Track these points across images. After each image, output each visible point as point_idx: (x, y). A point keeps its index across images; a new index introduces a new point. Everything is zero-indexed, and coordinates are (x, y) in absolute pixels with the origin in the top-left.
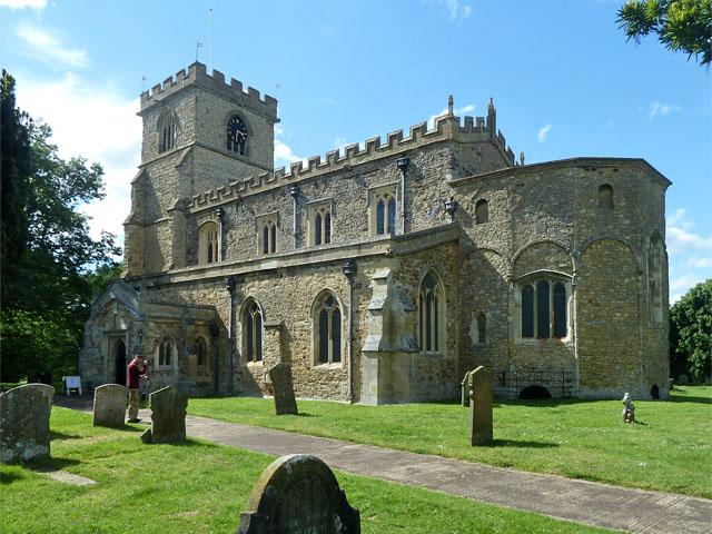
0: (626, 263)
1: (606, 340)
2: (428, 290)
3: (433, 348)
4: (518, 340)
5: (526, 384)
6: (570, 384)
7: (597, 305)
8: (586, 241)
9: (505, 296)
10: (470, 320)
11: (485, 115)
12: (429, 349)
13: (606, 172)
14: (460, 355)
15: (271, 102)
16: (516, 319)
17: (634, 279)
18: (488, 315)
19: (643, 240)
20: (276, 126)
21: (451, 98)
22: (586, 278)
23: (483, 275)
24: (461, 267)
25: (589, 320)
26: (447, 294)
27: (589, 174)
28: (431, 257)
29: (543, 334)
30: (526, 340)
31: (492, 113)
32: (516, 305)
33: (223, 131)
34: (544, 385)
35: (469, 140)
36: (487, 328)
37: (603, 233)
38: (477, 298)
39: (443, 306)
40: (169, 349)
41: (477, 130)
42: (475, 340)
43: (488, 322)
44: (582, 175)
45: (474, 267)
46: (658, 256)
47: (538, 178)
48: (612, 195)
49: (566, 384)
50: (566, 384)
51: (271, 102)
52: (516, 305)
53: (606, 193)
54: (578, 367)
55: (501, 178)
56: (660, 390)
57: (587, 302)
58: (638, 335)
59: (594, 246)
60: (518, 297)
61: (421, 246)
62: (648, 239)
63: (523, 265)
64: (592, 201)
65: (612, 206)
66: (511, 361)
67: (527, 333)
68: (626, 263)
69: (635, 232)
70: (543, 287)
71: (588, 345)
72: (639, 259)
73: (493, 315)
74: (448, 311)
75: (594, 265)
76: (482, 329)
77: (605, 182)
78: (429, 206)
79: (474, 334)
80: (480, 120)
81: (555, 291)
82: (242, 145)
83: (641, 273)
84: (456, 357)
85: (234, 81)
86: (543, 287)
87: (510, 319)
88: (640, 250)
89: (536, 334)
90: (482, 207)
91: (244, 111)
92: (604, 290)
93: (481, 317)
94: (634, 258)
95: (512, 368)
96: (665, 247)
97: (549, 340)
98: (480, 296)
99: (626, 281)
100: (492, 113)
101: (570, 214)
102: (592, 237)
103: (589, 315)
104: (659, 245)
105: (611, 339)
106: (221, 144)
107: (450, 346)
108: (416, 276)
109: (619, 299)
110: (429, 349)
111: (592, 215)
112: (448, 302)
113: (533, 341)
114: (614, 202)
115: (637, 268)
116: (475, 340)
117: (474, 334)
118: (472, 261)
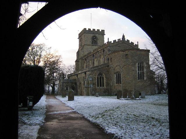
4: (116, 85)
11: (121, 38)
13: (127, 52)
15: (103, 31)
16: (115, 80)
20: (105, 36)
25: (124, 80)
31: (124, 36)
33: (91, 40)
39: (104, 78)
40: (68, 87)
42: (111, 85)
51: (103, 31)
67: (117, 83)
82: (96, 43)
85: (93, 29)
86: (118, 74)
91: (97, 35)
100: (124, 36)
106: (90, 44)
107: (107, 86)
110: (101, 86)
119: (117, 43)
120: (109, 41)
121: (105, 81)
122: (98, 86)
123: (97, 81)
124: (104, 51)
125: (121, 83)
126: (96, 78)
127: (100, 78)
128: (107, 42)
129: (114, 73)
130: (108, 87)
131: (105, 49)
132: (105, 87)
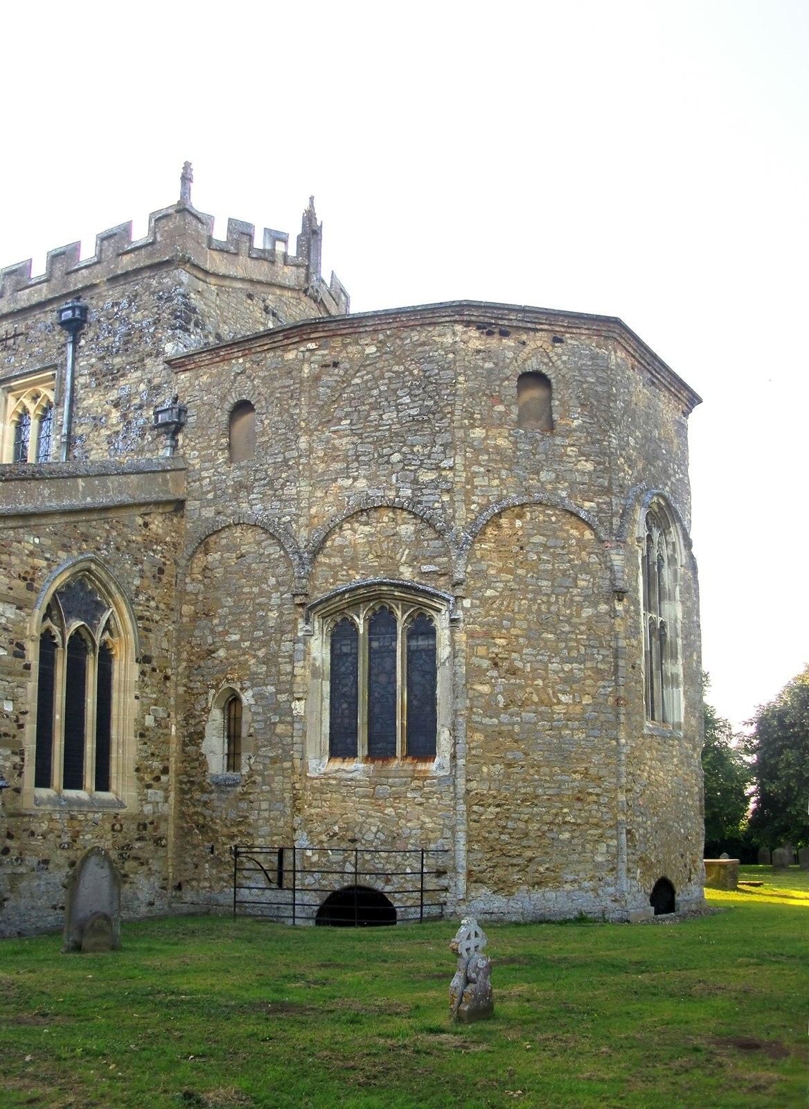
0: (585, 568)
1: (536, 766)
2: (76, 624)
3: (89, 779)
5: (335, 883)
6: (444, 882)
7: (513, 672)
8: (483, 508)
9: (287, 646)
10: (207, 711)
12: (73, 779)
13: (538, 341)
14: (181, 802)
17: (603, 608)
18: (247, 698)
19: (626, 514)
21: (187, 167)
22: (484, 601)
23: (236, 593)
24: (188, 571)
26: (142, 641)
27: (493, 342)
28: (86, 538)
29: (380, 751)
30: (337, 764)
32: (316, 673)
34: (379, 885)
35: (240, 273)
36: (244, 734)
37: (528, 491)
38: (222, 653)
39: (125, 670)
41: (267, 257)
42: (216, 764)
43: (246, 717)
44: (476, 344)
45: (219, 573)
46: (673, 560)
47: (371, 350)
48: (550, 398)
49: (431, 883)
50: (431, 883)
52: (316, 673)
53: (535, 394)
54: (461, 836)
55: (285, 348)
56: (678, 889)
57: (486, 664)
58: (617, 751)
59: (504, 521)
60: (320, 650)
61: (54, 504)
62: (640, 515)
63: (331, 567)
64: (501, 408)
65: (551, 425)
66: (298, 820)
67: (341, 746)
68: (585, 568)
69: (607, 491)
70: (382, 622)
71: (490, 778)
72: (617, 559)
73: (259, 697)
74: (142, 685)
75: (510, 571)
76: (233, 736)
77: (532, 365)
78: (124, 416)
79: (214, 746)
80: (276, 237)
81: (411, 635)
83: (620, 594)
84: (169, 809)
86: (382, 622)
87: (299, 707)
88: (620, 537)
89: (362, 750)
90: (245, 420)
92: (532, 638)
93: (232, 703)
94: (604, 555)
95: (302, 840)
96: (688, 544)
97: (395, 764)
98: (229, 647)
99: (587, 612)
101: (446, 437)
102: (500, 498)
103: (493, 695)
104: (675, 535)
105: (549, 764)
107: (148, 777)
108: (29, 581)
109: (570, 660)
111: (501, 442)
112: (145, 659)
113: (356, 768)
114: (555, 416)
115: (613, 581)
116: (216, 764)
117: (214, 746)
118: (214, 557)
119: (260, 271)
120: (198, 203)
121: (125, 707)
122: (43, 779)
123: (32, 685)
124: (75, 327)
125: (423, 747)
126: (32, 653)
127: (78, 645)
128: (159, 219)
129: (309, 609)
130: (155, 794)
131: (102, 304)
132: (124, 788)
